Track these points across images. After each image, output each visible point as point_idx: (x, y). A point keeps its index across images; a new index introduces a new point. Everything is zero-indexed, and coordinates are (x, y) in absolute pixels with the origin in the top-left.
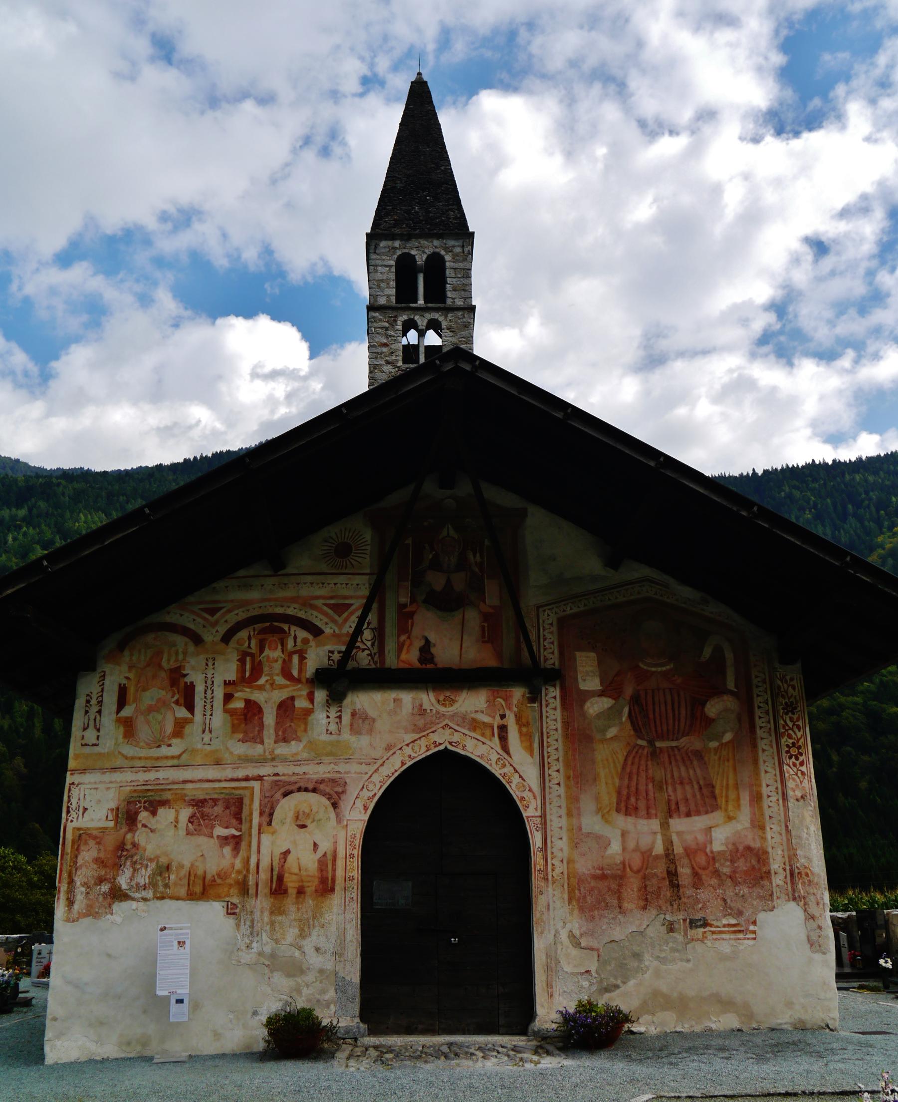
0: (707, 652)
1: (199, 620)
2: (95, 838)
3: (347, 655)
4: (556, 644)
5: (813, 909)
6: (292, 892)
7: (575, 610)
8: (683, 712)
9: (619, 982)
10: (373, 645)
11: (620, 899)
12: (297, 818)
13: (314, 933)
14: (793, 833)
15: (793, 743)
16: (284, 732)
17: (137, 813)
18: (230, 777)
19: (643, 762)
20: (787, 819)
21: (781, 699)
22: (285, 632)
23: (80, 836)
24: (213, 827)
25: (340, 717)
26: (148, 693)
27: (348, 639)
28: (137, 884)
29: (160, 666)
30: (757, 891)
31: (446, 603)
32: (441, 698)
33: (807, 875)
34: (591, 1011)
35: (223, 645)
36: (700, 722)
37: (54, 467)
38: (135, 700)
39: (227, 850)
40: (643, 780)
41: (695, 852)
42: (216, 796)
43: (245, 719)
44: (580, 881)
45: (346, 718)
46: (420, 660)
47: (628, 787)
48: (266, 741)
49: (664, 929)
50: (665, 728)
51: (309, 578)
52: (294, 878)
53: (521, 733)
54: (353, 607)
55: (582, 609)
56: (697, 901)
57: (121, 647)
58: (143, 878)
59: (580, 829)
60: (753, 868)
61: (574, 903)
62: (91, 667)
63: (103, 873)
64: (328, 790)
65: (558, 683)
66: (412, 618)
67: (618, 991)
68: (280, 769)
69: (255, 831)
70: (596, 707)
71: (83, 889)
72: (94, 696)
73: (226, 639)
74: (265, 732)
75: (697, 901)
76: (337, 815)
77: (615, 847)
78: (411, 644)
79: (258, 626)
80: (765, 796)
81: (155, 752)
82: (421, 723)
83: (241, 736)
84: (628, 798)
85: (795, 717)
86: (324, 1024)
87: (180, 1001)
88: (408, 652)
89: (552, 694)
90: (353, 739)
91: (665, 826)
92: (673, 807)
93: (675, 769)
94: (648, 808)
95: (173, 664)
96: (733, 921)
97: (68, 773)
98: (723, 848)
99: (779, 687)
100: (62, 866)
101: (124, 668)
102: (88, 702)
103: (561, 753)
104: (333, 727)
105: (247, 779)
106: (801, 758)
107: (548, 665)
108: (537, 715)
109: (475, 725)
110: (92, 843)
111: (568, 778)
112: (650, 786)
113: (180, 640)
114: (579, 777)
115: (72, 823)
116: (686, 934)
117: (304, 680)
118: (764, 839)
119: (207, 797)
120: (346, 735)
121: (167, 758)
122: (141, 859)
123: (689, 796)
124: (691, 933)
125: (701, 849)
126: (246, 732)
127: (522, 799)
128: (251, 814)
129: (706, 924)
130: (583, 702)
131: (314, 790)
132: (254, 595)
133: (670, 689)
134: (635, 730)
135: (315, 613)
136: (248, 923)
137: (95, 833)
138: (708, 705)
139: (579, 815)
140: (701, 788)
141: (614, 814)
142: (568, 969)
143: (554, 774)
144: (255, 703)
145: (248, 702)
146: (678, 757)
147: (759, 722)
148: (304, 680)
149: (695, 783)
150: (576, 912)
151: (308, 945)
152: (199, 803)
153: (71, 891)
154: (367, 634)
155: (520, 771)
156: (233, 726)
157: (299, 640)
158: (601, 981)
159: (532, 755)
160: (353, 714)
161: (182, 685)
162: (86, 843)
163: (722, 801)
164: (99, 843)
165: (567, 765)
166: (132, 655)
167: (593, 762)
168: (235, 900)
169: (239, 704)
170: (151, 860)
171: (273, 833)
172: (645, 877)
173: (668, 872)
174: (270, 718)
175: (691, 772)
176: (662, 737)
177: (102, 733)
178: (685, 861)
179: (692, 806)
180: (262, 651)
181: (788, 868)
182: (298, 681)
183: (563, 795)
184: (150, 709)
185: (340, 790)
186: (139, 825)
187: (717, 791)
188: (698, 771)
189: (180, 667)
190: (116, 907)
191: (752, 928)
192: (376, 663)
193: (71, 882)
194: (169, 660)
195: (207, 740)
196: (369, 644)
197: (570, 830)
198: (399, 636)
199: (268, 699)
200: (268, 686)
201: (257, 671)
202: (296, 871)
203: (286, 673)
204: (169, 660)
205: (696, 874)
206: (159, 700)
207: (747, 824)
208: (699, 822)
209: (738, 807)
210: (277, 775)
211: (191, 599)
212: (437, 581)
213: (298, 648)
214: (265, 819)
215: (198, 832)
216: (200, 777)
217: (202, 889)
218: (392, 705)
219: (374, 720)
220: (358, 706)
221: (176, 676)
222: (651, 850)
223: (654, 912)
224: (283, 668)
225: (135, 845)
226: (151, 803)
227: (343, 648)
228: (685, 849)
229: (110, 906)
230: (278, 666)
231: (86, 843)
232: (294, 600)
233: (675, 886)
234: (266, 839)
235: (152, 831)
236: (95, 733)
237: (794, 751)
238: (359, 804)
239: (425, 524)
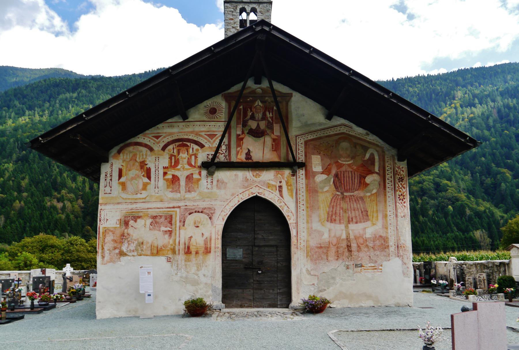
0: (367, 156)
1: (152, 141)
2: (112, 231)
3: (215, 156)
4: (304, 152)
5: (405, 260)
6: (194, 253)
7: (312, 138)
8: (356, 180)
9: (326, 288)
10: (226, 152)
11: (327, 256)
12: (195, 223)
13: (203, 269)
14: (399, 230)
15: (402, 194)
16: (189, 188)
17: (129, 221)
18: (167, 206)
19: (339, 201)
20: (397, 225)
21: (397, 176)
22: (188, 146)
23: (106, 230)
24: (160, 227)
25: (212, 182)
26: (131, 172)
27: (215, 149)
28: (130, 250)
29: (136, 160)
30: (383, 253)
31: (257, 134)
32: (255, 174)
33: (404, 247)
34: (314, 299)
35: (162, 151)
36: (363, 185)
37: (88, 75)
38: (126, 175)
39: (167, 236)
40: (338, 208)
41: (359, 238)
42: (161, 214)
43: (172, 183)
44: (311, 249)
45: (215, 182)
46: (246, 159)
47: (332, 211)
48: (181, 192)
49: (345, 268)
50: (348, 187)
51: (198, 123)
52: (194, 247)
53: (288, 189)
54: (217, 136)
55: (315, 137)
56: (359, 257)
57: (119, 152)
58: (132, 247)
59: (312, 228)
60: (382, 244)
61: (309, 257)
62: (107, 161)
63: (116, 245)
64: (207, 212)
65: (304, 168)
67: (325, 292)
68: (187, 204)
69: (178, 229)
70: (320, 178)
71: (108, 252)
72: (109, 173)
73: (164, 149)
74: (181, 188)
75: (359, 257)
76: (212, 222)
77: (326, 236)
78: (242, 152)
79: (177, 144)
80: (388, 215)
81: (135, 196)
82: (246, 185)
83: (171, 190)
84: (332, 216)
85: (403, 183)
86: (207, 304)
87: (149, 295)
88: (241, 154)
89: (301, 172)
90: (218, 191)
91: (347, 227)
92: (350, 219)
93: (352, 204)
94: (340, 220)
95: (141, 160)
96: (373, 265)
97: (99, 205)
98: (370, 236)
99: (397, 171)
100: (99, 242)
101: (121, 161)
102: (106, 175)
103: (304, 198)
104: (209, 186)
105: (174, 208)
106: (404, 200)
107: (300, 161)
108: (295, 181)
109: (269, 186)
110: (111, 233)
111: (307, 207)
112: (341, 211)
113: (144, 149)
114: (312, 207)
115: (102, 225)
116: (353, 270)
117: (197, 167)
118: (387, 233)
119: (157, 215)
120: (215, 190)
121: (140, 199)
122: (131, 239)
123: (357, 215)
124: (355, 269)
125: (361, 236)
126: (173, 188)
127: (288, 216)
128: (176, 222)
129: (362, 266)
130: (314, 176)
131: (202, 212)
132: (175, 130)
133: (351, 172)
134: (336, 188)
135: (201, 138)
136: (176, 265)
137: (112, 229)
138: (367, 178)
139: (311, 223)
140: (362, 212)
141: (326, 222)
142: (305, 283)
143: (302, 206)
144: (176, 176)
145: (173, 175)
146: (354, 200)
147: (387, 185)
148: (197, 167)
149: (360, 210)
150: (309, 261)
151: (201, 273)
152: (154, 217)
153: (103, 252)
154: (223, 147)
155: (287, 205)
156: (167, 185)
157: (194, 150)
158: (319, 288)
159: (292, 198)
160: (218, 181)
161: (145, 169)
162: (108, 233)
163: (370, 217)
164: (113, 233)
165: (307, 202)
166: (124, 156)
167: (318, 201)
168: (170, 256)
169: (169, 177)
170: (135, 240)
171: (185, 229)
172: (337, 248)
173: (347, 246)
174: (183, 182)
175: (358, 205)
176: (347, 191)
177: (112, 188)
178: (355, 241)
179: (358, 220)
180: (179, 154)
181: (396, 244)
182: (195, 167)
183: (305, 215)
184: (132, 179)
185: (212, 212)
186: (130, 226)
187: (369, 213)
188: (361, 205)
189: (144, 161)
190: (122, 258)
191: (380, 268)
192: (227, 160)
193: (103, 249)
194: (139, 158)
195: (156, 191)
196: (224, 151)
197: (308, 229)
198: (237, 148)
199: (182, 174)
200: (182, 169)
201: (177, 162)
202: (195, 244)
203: (190, 164)
204: (139, 158)
205: (359, 246)
206: (136, 175)
207: (381, 227)
208: (361, 226)
209: (377, 219)
210: (186, 206)
211: (147, 132)
212: (253, 124)
213: (194, 153)
214: (182, 224)
215: (154, 229)
216: (154, 207)
217: (157, 252)
218: (234, 177)
219: (226, 183)
220: (220, 178)
221: (143, 164)
222: (340, 237)
223: (341, 261)
224: (188, 162)
225: (128, 234)
226: (134, 217)
227: (213, 153)
228: (355, 237)
229: (119, 258)
230: (186, 161)
231: (108, 233)
232: (192, 132)
233: (350, 251)
234: (182, 231)
235: (135, 228)
236: (110, 189)
237: (401, 197)
238: (221, 218)
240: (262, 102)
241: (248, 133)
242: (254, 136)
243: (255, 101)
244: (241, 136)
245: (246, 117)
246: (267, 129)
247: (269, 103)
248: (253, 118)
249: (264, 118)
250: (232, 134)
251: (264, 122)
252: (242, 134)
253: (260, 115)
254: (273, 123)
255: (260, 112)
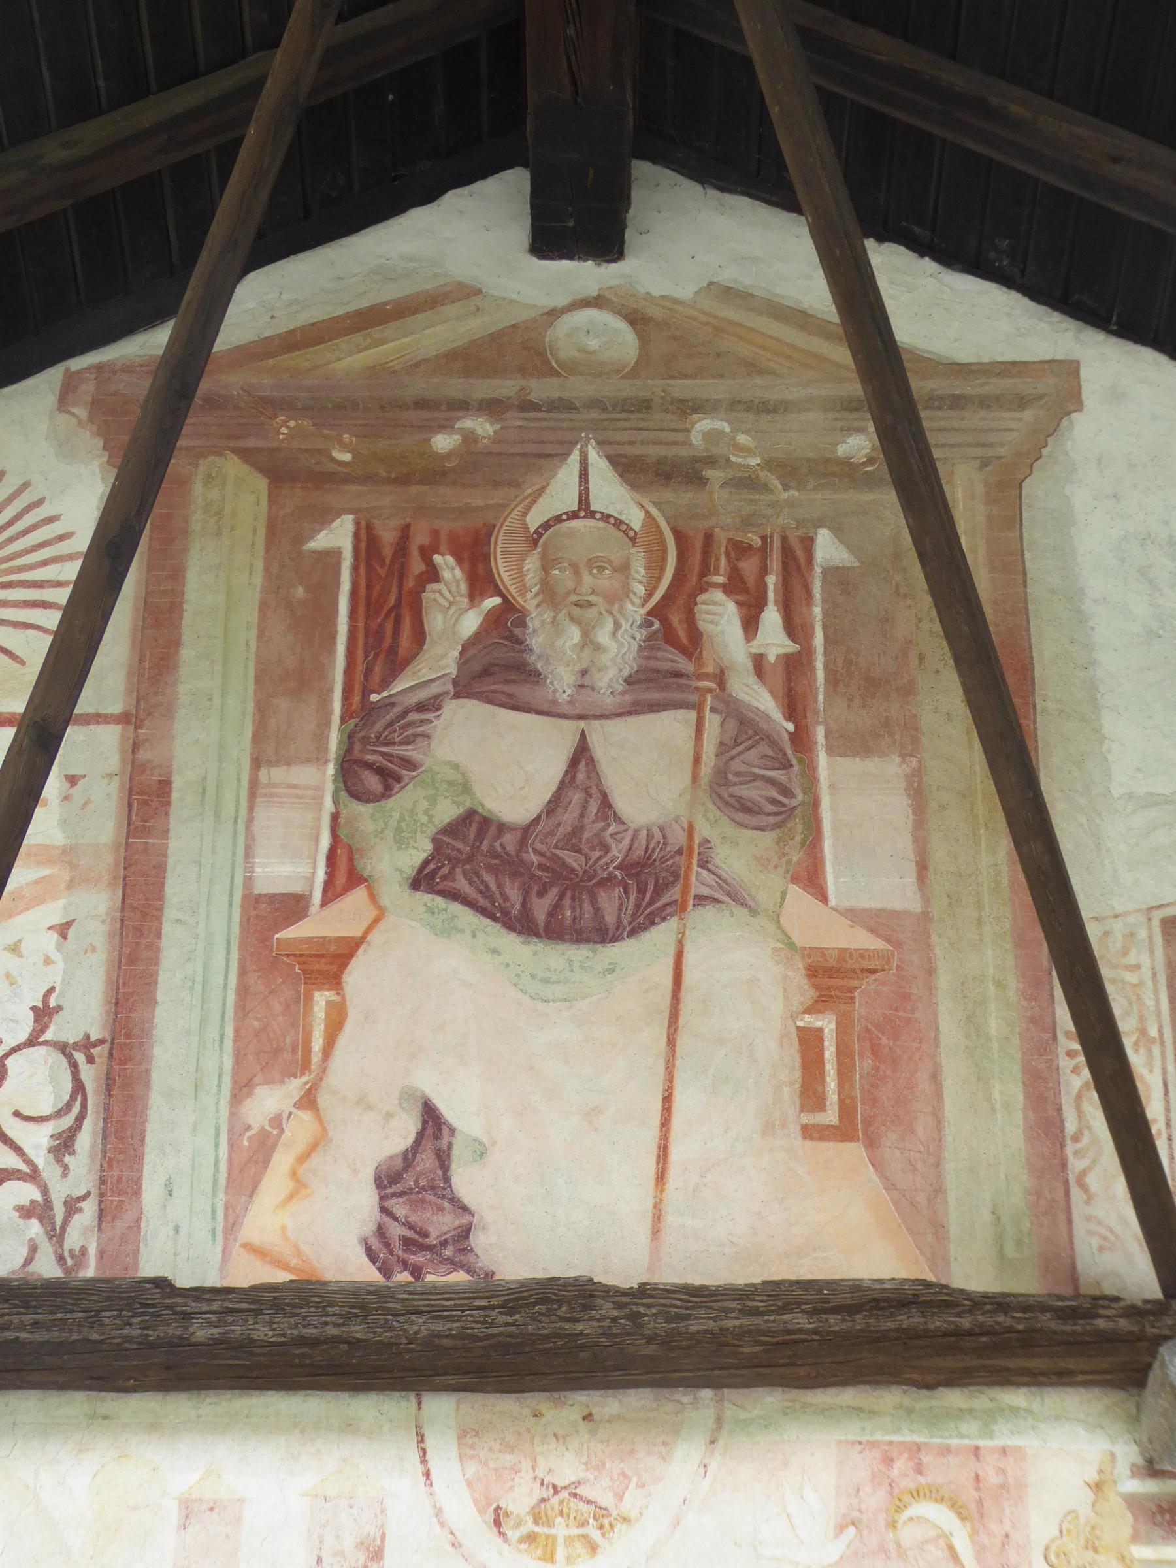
10: (64, 1145)
32: (520, 1499)
66: (334, 981)
88: (299, 1185)
196: (37, 1141)
198: (242, 1089)
212: (501, 763)
239: (443, 442)
240: (628, 468)
241: (423, 880)
242: (522, 925)
243: (547, 457)
244: (318, 925)
245: (397, 664)
246: (712, 826)
247: (747, 483)
248: (501, 670)
249: (671, 668)
250: (179, 888)
251: (673, 727)
252: (331, 892)
253: (618, 644)
254: (801, 739)
255: (615, 599)
